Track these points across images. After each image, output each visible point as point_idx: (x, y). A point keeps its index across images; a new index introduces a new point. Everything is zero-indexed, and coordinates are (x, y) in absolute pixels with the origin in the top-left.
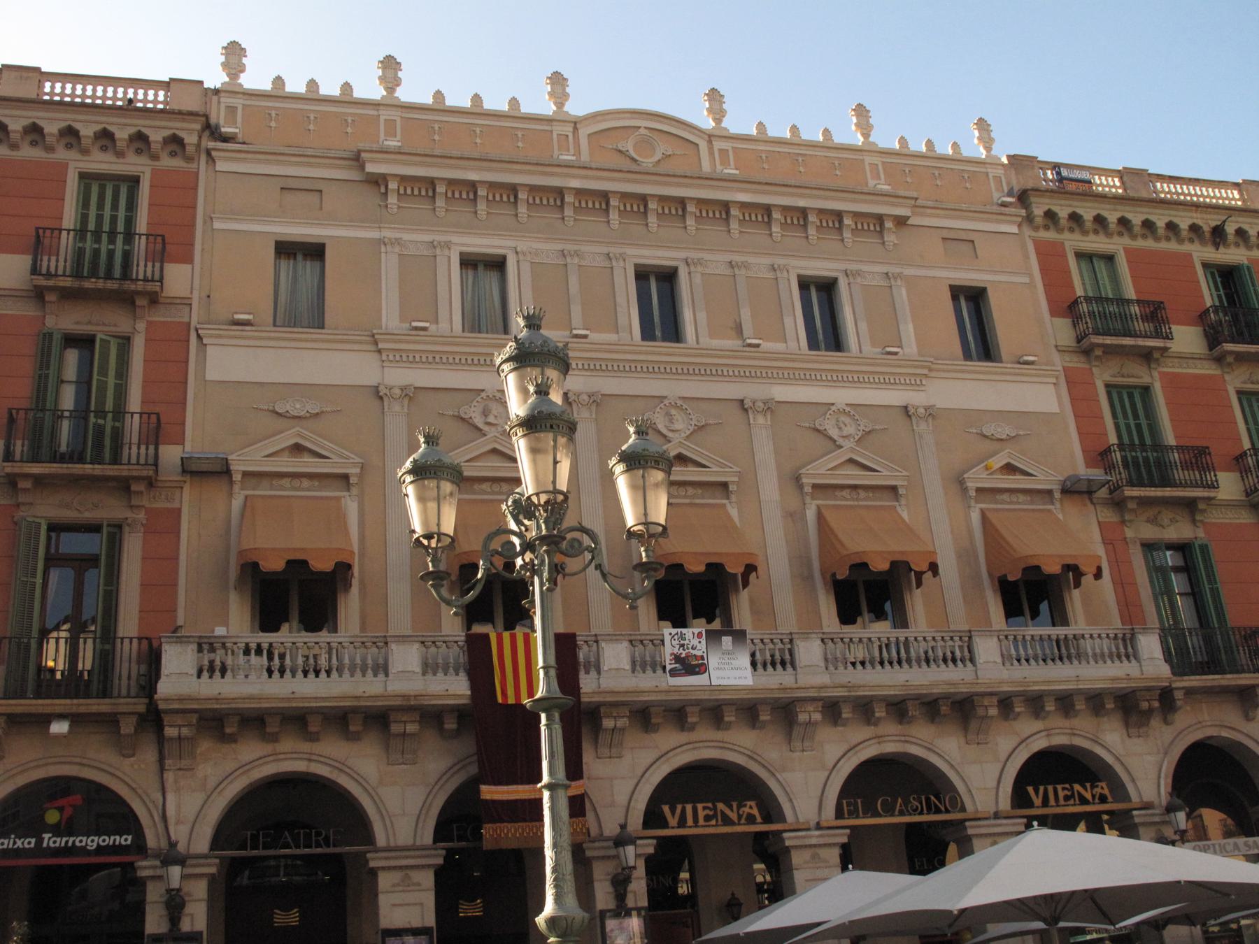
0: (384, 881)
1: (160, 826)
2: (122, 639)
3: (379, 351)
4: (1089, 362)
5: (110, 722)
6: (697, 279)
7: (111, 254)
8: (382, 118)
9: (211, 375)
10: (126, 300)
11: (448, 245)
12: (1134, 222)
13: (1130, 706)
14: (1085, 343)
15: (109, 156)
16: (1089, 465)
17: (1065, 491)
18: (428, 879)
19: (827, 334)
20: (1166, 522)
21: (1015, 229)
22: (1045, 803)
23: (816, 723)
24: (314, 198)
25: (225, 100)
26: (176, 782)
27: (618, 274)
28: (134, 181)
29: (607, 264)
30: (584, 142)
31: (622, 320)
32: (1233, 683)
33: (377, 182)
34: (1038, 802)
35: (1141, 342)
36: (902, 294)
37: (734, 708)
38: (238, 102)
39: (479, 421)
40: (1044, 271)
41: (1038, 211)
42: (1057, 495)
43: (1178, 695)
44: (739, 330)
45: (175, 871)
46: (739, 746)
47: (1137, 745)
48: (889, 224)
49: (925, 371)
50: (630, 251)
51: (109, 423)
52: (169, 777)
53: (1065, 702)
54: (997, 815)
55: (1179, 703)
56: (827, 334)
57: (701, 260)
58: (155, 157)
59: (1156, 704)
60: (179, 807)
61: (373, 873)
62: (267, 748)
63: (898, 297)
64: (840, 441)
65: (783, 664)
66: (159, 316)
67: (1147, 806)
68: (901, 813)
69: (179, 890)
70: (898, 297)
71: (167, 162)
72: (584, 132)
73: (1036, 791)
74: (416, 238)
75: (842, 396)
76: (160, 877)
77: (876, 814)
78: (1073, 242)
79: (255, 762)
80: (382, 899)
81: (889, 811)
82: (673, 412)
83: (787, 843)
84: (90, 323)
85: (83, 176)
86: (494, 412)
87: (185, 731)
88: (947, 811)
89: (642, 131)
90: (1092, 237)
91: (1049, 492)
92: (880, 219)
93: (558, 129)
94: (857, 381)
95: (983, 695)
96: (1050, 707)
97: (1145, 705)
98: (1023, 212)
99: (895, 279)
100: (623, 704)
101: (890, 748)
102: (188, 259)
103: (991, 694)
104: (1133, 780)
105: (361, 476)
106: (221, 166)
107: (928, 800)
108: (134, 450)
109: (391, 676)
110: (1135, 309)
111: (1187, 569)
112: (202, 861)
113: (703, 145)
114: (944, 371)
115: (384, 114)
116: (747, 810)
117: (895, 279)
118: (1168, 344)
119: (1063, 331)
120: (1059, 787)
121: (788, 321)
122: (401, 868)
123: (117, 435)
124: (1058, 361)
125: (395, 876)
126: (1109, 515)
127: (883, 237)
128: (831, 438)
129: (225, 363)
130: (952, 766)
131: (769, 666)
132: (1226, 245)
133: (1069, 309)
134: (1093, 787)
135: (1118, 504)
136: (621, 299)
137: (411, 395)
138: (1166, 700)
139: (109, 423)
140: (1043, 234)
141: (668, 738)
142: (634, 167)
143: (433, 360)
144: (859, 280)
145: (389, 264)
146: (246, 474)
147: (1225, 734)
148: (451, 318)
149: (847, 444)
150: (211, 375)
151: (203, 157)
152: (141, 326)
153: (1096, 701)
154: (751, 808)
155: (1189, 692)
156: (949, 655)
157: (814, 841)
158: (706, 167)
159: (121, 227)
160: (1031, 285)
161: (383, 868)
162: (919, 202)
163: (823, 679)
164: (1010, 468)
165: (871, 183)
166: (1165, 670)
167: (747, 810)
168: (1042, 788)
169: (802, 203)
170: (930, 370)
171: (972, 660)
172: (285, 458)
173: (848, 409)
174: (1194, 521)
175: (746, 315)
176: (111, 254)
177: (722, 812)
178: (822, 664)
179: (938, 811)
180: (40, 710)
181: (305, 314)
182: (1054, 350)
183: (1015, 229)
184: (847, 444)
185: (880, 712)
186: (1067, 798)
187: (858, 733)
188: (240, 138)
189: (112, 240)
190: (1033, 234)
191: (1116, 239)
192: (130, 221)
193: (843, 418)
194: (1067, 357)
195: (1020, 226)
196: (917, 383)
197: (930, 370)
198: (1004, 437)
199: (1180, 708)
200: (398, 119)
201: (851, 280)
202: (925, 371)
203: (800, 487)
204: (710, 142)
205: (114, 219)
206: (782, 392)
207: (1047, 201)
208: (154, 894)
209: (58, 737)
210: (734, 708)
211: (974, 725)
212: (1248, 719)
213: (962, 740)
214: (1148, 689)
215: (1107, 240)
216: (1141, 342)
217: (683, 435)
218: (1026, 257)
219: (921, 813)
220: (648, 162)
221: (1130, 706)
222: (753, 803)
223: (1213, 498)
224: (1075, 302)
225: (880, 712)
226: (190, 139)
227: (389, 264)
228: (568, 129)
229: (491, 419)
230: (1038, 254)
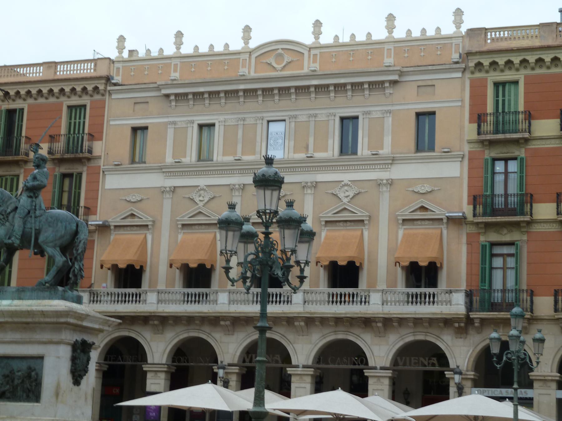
9: (107, 186)
11: (192, 122)
19: (348, 146)
28: (85, 106)
31: (258, 149)
33: (167, 96)
36: (389, 121)
40: (472, 97)
44: (307, 148)
50: (264, 115)
56: (348, 146)
58: (91, 96)
63: (386, 124)
68: (339, 364)
70: (386, 124)
73: (401, 359)
74: (180, 120)
75: (346, 177)
77: (328, 364)
81: (334, 362)
83: (447, 376)
86: (203, 195)
88: (359, 365)
105: (153, 225)
116: (276, 358)
121: (330, 142)
133: (479, 118)
134: (429, 359)
138: (469, 321)
145: (170, 133)
150: (107, 186)
157: (299, 373)
160: (462, 107)
167: (276, 358)
168: (404, 358)
173: (349, 183)
175: (311, 140)
181: (136, 159)
183: (459, 75)
186: (415, 363)
194: (472, 145)
206: (321, 177)
218: (463, 90)
226: (101, 87)
227: (170, 133)
230: (471, 87)
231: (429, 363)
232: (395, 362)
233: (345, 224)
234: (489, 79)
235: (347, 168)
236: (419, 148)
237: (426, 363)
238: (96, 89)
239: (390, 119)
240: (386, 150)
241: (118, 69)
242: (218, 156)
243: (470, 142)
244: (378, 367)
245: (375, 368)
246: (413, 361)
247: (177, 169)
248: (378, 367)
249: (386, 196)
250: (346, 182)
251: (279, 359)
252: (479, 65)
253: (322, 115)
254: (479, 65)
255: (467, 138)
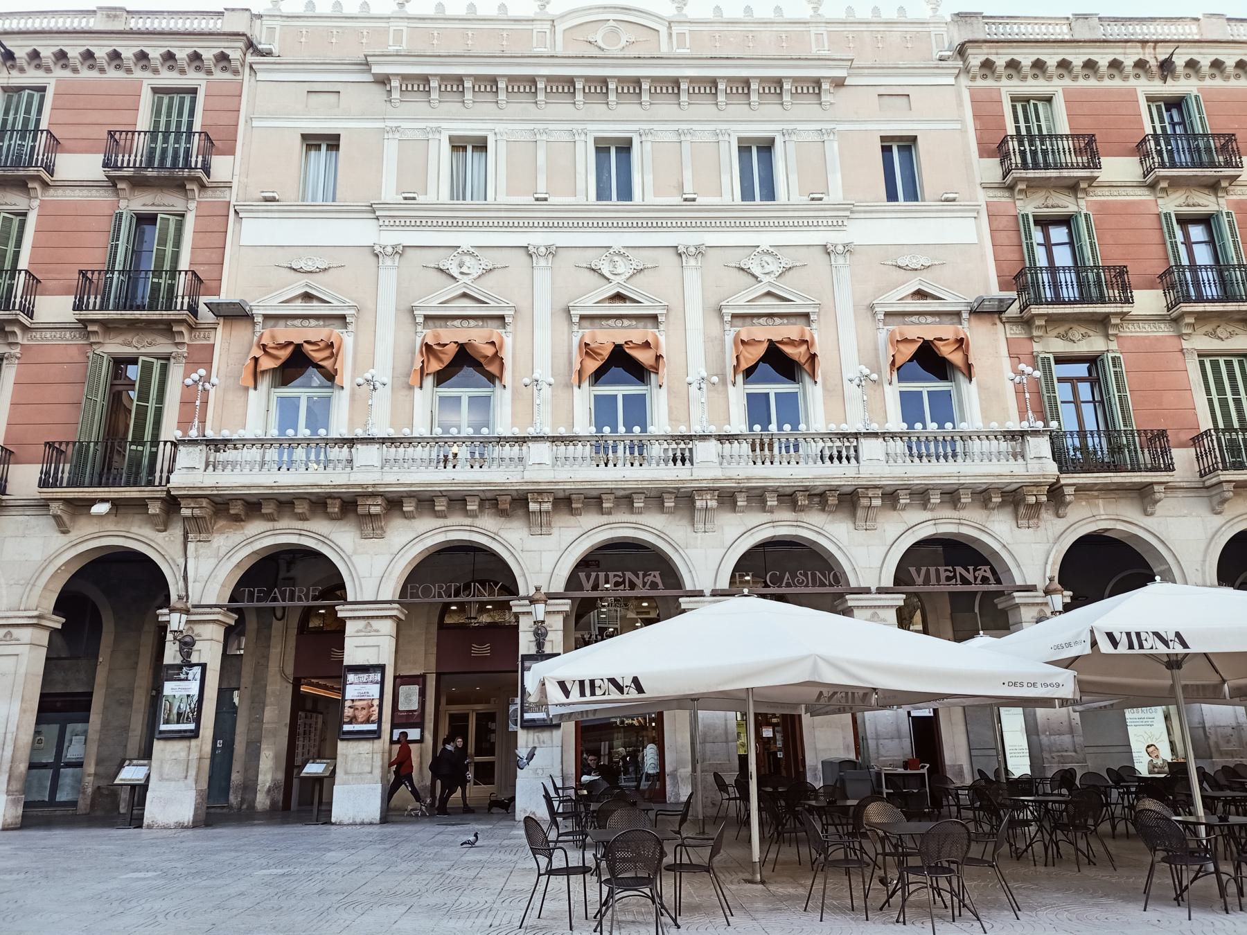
0: (350, 627)
1: (181, 583)
2: (165, 442)
3: (377, 218)
4: (1012, 196)
5: (140, 505)
6: (648, 146)
7: (164, 151)
8: (392, 29)
10: (180, 186)
11: (438, 130)
12: (1074, 63)
13: (1013, 499)
14: (1009, 179)
15: (175, 74)
16: (1003, 286)
17: (973, 312)
18: (388, 627)
20: (1077, 336)
21: (951, 81)
22: (927, 581)
23: (712, 509)
24: (333, 97)
25: (267, 22)
26: (196, 550)
27: (580, 147)
28: (194, 91)
29: (570, 139)
30: (559, 37)
31: (580, 185)
32: (1128, 480)
33: (383, 80)
34: (920, 580)
35: (1065, 173)
36: (833, 147)
37: (643, 496)
38: (277, 23)
39: (455, 271)
41: (975, 60)
42: (965, 315)
43: (1069, 491)
45: (540, 609)
46: (650, 527)
47: (1026, 534)
48: (825, 86)
49: (847, 213)
50: (590, 127)
51: (164, 281)
52: (191, 546)
53: (952, 496)
54: (881, 591)
55: (1068, 498)
57: (651, 128)
58: (209, 72)
59: (1044, 499)
60: (196, 568)
61: (342, 622)
62: (268, 525)
63: (828, 152)
64: (761, 277)
65: (683, 460)
66: (208, 197)
67: (1032, 588)
68: (788, 585)
69: (543, 622)
71: (218, 75)
72: (560, 28)
73: (919, 572)
75: (766, 239)
76: (529, 613)
78: (1009, 87)
79: (260, 536)
80: (348, 643)
82: (616, 258)
84: (153, 205)
85: (156, 90)
86: (467, 264)
87: (197, 512)
88: (831, 585)
89: (611, 23)
90: (1030, 81)
91: (958, 314)
92: (818, 82)
93: (537, 27)
94: (782, 224)
95: (867, 488)
96: (935, 499)
97: (1032, 500)
98: (960, 64)
99: (828, 134)
100: (549, 492)
101: (783, 531)
102: (232, 152)
103: (876, 487)
104: (1019, 566)
106: (260, 76)
107: (814, 576)
108: (182, 301)
109: (355, 469)
110: (1067, 144)
111: (1095, 380)
112: (208, 610)
113: (664, 31)
114: (865, 212)
115: (394, 25)
116: (651, 578)
117: (828, 134)
118: (1096, 173)
119: (991, 169)
120: (942, 569)
121: (725, 179)
122: (364, 618)
123: (171, 289)
124: (982, 197)
125: (361, 624)
126: (1016, 332)
127: (820, 98)
128: (753, 275)
129: (252, 233)
130: (840, 548)
131: (679, 462)
132: (1175, 77)
133: (1001, 152)
135: (1026, 322)
136: (580, 168)
137: (400, 251)
139: (164, 281)
140: (980, 83)
141: (590, 520)
142: (600, 54)
143: (420, 224)
144: (794, 138)
145: (391, 148)
146: (266, 317)
147: (1120, 526)
148: (438, 191)
149: (766, 279)
151: (247, 70)
152: (192, 205)
153: (983, 496)
154: (655, 576)
155: (1080, 489)
156: (835, 454)
158: (664, 49)
159: (184, 129)
160: (963, 131)
161: (350, 618)
162: (855, 64)
163: (717, 473)
164: (920, 294)
165: (814, 50)
166: (1052, 468)
167: (651, 578)
168: (924, 569)
169: (744, 73)
170: (852, 212)
171: (857, 459)
172: (298, 303)
174: (1107, 336)
176: (164, 151)
177: (630, 581)
178: (716, 460)
179: (822, 585)
180: (87, 496)
182: (979, 189)
183: (951, 81)
184: (766, 279)
185: (772, 502)
186: (948, 579)
187: (915, 516)
188: (275, 51)
189: (166, 140)
190: (970, 84)
191: (1056, 81)
192: (190, 124)
193: (766, 258)
194: (991, 193)
195: (957, 76)
196: (838, 224)
197: (852, 212)
198: (918, 267)
199: (1070, 503)
200: (405, 29)
201: (787, 138)
202: (847, 213)
203: (721, 316)
204: (670, 27)
205: (179, 123)
207: (986, 51)
208: (525, 625)
209: (100, 517)
210: (643, 496)
211: (860, 513)
212: (1146, 514)
213: (851, 526)
214: (1037, 485)
215: (1046, 83)
216: (1065, 173)
217: (624, 277)
218: (960, 104)
219: (807, 586)
220: (614, 50)
221: (1013, 499)
222: (657, 573)
223: (1126, 314)
224: (1004, 141)
225: (772, 502)
226: (234, 55)
227: (391, 148)
228: (547, 26)
229: (464, 270)
231: (976, 578)
232: (902, 577)
233: (770, 321)
234: (1003, 90)
235: (763, 224)
236: (892, 196)
237: (970, 577)
238: (223, 57)
239: (836, 145)
240: (836, 194)
241: (271, 29)
242: (500, 192)
243: (985, 187)
244: (873, 589)
245: (867, 591)
246: (943, 575)
247: (409, 211)
248: (873, 589)
249: (845, 273)
250: (765, 247)
251: (658, 580)
252: (987, 65)
253: (704, 132)
254: (987, 65)
255: (978, 181)
